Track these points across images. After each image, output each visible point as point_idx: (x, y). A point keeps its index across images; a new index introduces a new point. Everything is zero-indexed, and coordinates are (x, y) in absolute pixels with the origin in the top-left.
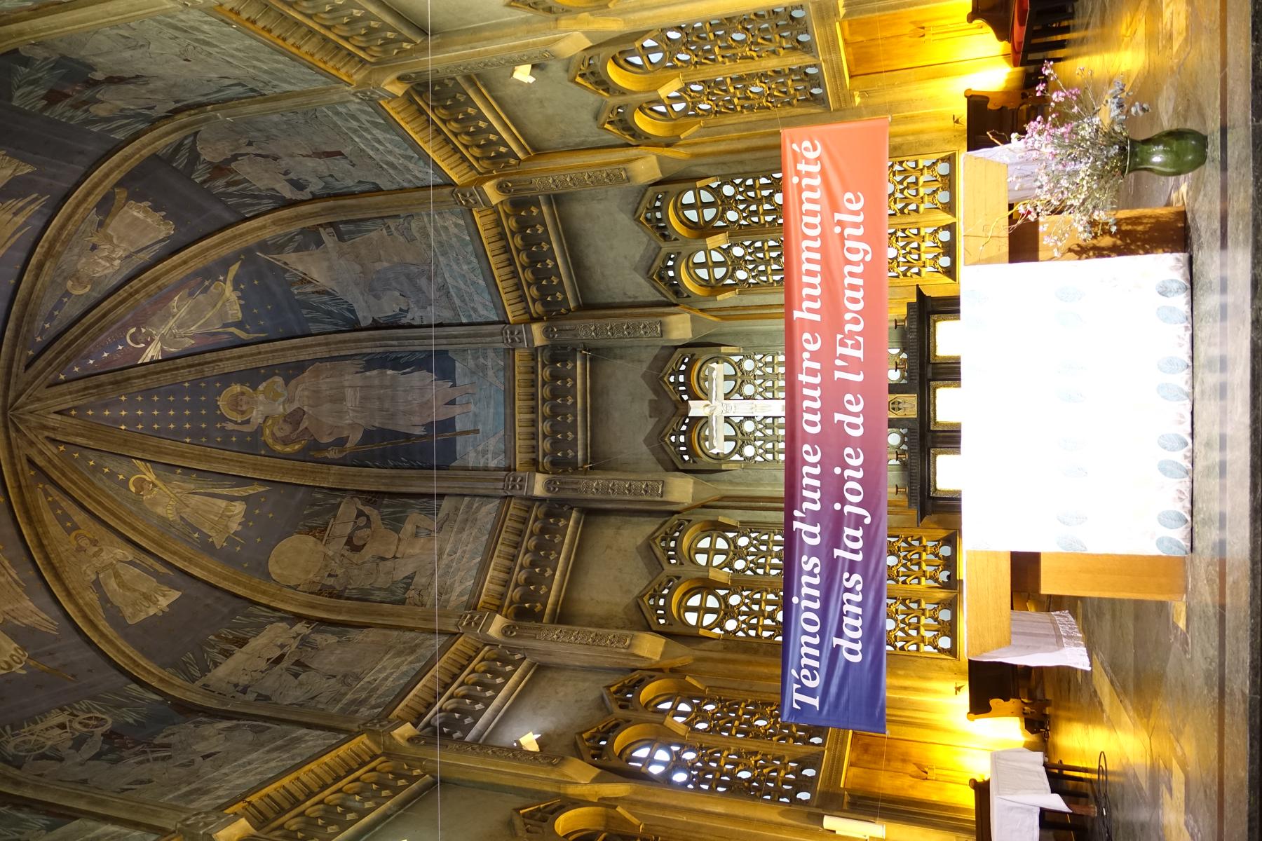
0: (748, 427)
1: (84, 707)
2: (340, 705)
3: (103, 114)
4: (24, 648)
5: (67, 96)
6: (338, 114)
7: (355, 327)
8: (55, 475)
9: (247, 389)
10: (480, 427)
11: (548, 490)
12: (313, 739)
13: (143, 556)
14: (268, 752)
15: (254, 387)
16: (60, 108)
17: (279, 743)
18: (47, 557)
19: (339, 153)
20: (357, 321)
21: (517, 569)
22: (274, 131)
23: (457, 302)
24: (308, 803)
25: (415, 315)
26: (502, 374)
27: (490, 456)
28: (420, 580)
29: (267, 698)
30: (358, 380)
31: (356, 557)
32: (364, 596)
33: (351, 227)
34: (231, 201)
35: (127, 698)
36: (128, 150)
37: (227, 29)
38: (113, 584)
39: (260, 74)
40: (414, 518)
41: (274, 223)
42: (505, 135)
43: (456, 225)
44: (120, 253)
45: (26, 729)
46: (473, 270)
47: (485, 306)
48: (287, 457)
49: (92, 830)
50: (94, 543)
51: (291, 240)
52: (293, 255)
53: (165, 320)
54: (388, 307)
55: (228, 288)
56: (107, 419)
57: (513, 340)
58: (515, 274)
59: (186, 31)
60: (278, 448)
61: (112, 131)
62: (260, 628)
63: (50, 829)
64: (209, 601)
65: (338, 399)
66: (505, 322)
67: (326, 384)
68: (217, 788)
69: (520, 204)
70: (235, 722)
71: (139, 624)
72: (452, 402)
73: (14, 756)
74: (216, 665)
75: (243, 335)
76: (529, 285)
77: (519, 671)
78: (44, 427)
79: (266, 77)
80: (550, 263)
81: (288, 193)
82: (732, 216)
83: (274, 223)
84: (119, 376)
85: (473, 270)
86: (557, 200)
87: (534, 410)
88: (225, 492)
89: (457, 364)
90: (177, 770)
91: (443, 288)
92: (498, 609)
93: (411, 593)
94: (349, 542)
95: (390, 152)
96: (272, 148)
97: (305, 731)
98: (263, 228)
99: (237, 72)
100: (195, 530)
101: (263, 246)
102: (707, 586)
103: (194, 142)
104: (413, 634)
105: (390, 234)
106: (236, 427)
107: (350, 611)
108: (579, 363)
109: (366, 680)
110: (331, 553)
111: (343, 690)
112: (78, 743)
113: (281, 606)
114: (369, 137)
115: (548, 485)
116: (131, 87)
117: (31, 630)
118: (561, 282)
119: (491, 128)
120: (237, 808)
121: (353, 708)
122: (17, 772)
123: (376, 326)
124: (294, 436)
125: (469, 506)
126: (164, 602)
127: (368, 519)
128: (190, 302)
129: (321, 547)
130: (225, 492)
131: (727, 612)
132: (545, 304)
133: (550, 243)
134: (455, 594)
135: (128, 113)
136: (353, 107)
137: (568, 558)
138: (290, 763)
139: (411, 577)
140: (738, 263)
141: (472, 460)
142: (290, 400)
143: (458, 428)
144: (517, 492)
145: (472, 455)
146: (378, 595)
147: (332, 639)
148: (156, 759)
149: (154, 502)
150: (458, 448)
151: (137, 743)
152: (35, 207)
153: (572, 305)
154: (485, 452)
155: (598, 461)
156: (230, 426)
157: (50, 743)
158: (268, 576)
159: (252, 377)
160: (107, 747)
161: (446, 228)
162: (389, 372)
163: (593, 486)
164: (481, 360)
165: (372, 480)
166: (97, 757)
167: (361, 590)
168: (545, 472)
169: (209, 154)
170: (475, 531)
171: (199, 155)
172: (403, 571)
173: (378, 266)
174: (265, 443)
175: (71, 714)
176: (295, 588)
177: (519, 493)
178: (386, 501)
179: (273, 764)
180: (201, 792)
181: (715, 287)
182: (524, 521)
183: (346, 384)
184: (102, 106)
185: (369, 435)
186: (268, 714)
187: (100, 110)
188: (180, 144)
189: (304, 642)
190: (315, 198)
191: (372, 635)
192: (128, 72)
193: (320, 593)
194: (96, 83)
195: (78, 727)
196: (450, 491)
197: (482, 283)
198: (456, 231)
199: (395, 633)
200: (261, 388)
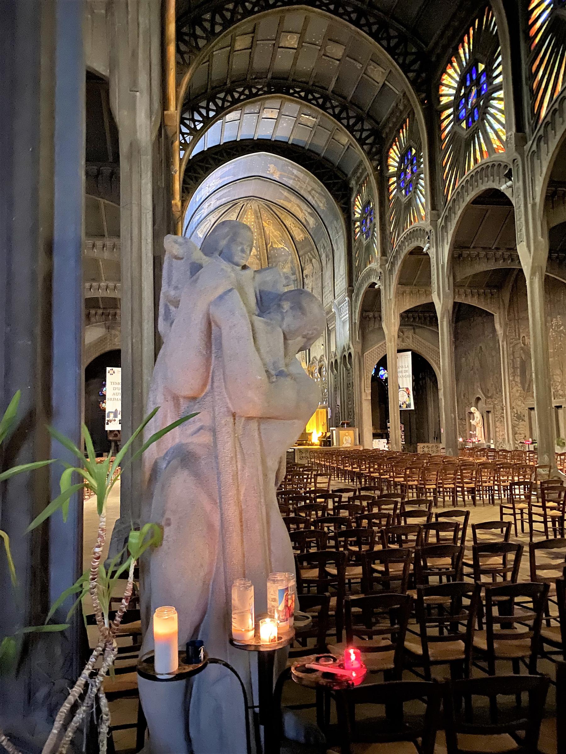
52: (289, 265)
53: (274, 229)
75: (269, 246)
84: (259, 217)
98: (297, 261)
169: (314, 260)
190: (303, 278)
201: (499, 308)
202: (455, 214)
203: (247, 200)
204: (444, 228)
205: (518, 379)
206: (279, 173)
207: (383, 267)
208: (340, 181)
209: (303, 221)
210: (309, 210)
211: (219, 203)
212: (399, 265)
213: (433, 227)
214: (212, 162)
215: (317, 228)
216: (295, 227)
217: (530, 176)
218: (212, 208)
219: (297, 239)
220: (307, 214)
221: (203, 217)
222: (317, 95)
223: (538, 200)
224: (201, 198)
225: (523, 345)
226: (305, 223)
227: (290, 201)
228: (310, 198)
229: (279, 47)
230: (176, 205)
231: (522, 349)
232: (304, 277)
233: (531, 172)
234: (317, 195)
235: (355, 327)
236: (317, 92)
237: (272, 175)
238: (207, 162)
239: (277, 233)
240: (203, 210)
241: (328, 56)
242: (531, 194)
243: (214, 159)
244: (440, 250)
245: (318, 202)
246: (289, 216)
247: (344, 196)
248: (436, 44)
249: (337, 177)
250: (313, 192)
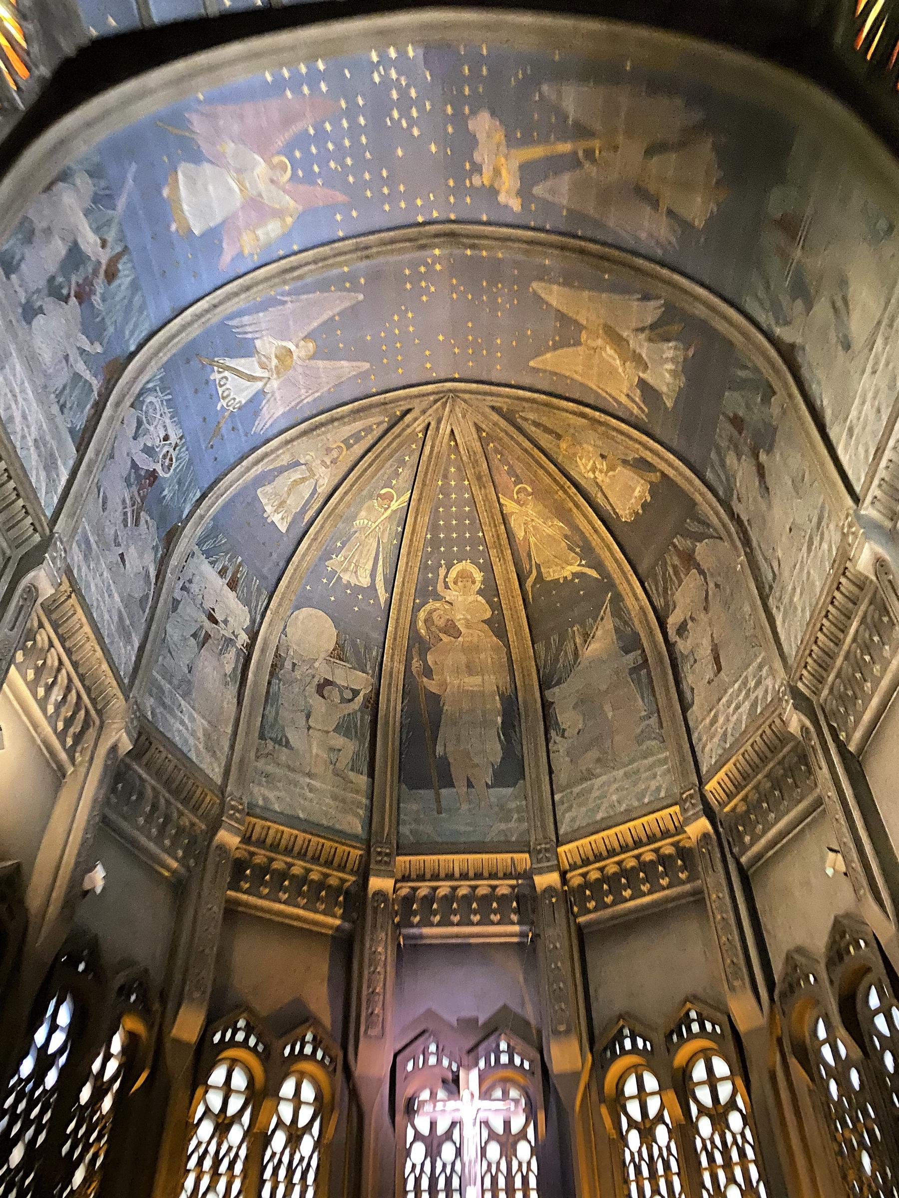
0: (448, 1151)
1: (182, 455)
2: (159, 678)
3: (728, 462)
4: (239, 408)
5: (740, 433)
6: (760, 667)
7: (544, 685)
8: (397, 430)
9: (478, 586)
11: (376, 893)
12: (126, 654)
13: (321, 500)
14: (120, 612)
15: (480, 592)
16: (728, 426)
17: (128, 622)
18: (322, 425)
19: (719, 669)
21: (289, 860)
22: (733, 607)
23: (576, 790)
24: (61, 650)
25: (560, 745)
26: (502, 838)
27: (413, 826)
28: (284, 755)
29: (175, 609)
31: (312, 689)
33: (644, 680)
34: (658, 569)
35: (187, 489)
36: (697, 482)
37: (827, 566)
38: (295, 475)
39: (787, 596)
40: (349, 747)
41: (641, 608)
42: (763, 842)
43: (658, 789)
44: (600, 477)
45: (166, 410)
46: (612, 806)
47: (573, 820)
48: (413, 623)
49: (64, 464)
50: (334, 462)
51: (626, 623)
55: (576, 569)
56: (447, 470)
57: (540, 852)
58: (612, 853)
59: (818, 528)
60: (422, 615)
61: (713, 467)
62: (246, 602)
63: (71, 431)
64: (275, 556)
65: (470, 669)
66: (559, 843)
67: (487, 657)
68: (89, 566)
70: (153, 581)
71: (256, 498)
72: (470, 785)
73: (143, 402)
74: (212, 563)
76: (601, 869)
78: (439, 421)
79: (786, 600)
80: (627, 893)
81: (673, 621)
82: (705, 1126)
83: (641, 608)
84: (486, 479)
85: (612, 806)
86: (698, 899)
88: (380, 569)
89: (511, 790)
90: (113, 532)
91: (589, 775)
92: (247, 839)
94: (328, 682)
95: (728, 720)
96: (715, 606)
97: (136, 645)
99: (786, 573)
100: (344, 544)
101: (618, 598)
103: (712, 537)
104: (226, 749)
105: (643, 719)
106: (441, 577)
107: (255, 683)
108: (516, 928)
109: (183, 702)
110: (317, 665)
111: (176, 682)
112: (149, 451)
113: (267, 619)
114: (741, 698)
115: (380, 894)
116: (757, 483)
117: (257, 413)
118: (607, 906)
120: (66, 586)
121: (155, 690)
122: (128, 404)
123: (546, 705)
124: (433, 629)
125: (359, 805)
126: (276, 518)
127: (350, 701)
128: (559, 537)
129: (323, 655)
130: (380, 569)
131: (222, 1127)
132: (582, 887)
133: (651, 892)
134: (267, 793)
135: (732, 480)
136: (769, 682)
137: (298, 918)
138: (105, 634)
139: (287, 745)
140: (647, 1136)
141: (411, 807)
143: (443, 791)
144: (374, 858)
145: (415, 807)
146: (271, 711)
147: (229, 669)
148: (125, 514)
149: (371, 509)
150: (422, 791)
151: (143, 499)
152: (636, 411)
153: (581, 920)
154: (417, 821)
156: (442, 571)
157: (152, 428)
158: (298, 607)
159: (490, 591)
160: (143, 473)
161: (655, 776)
162: (499, 719)
164: (515, 816)
166: (134, 465)
167: (277, 695)
168: (395, 891)
169: (701, 549)
170: (333, 812)
171: (701, 541)
172: (292, 736)
173: (607, 708)
175: (176, 445)
176: (284, 632)
177: (372, 861)
178: (368, 718)
179: (106, 617)
180: (87, 553)
181: (618, 1102)
182: (342, 868)
183: (486, 677)
184: (735, 461)
185: (435, 699)
186: (158, 611)
187: (731, 459)
188: (709, 526)
189: (229, 642)
191: (229, 705)
192: (770, 481)
193: (277, 655)
194: (756, 456)
195: (165, 451)
197: (599, 817)
198: (653, 788)
199: (229, 730)
200: (480, 598)
239: (554, 528)
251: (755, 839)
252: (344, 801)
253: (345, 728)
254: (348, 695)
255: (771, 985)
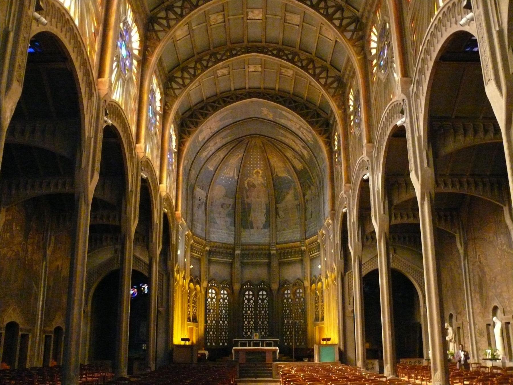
7: (277, 202)
10: (251, 236)
15: (261, 176)
20: (278, 203)
28: (216, 225)
30: (263, 202)
32: (211, 211)
40: (229, 220)
44: (292, 159)
54: (281, 213)
55: (286, 175)
60: (246, 182)
69: (302, 252)
72: (258, 229)
77: (198, 255)
81: (307, 197)
86: (302, 261)
87: (256, 250)
88: (235, 172)
91: (284, 230)
93: (212, 223)
94: (224, 204)
102: (216, 294)
115: (238, 254)
118: (285, 259)
119: (315, 253)
123: (277, 208)
125: (232, 234)
142: (258, 184)
143: (252, 230)
147: (203, 210)
155: (243, 265)
162: (265, 211)
163: (237, 265)
165: (239, 207)
169: (312, 187)
174: (246, 179)
178: (233, 211)
182: (230, 249)
185: (249, 205)
196: (236, 229)
197: (285, 240)
201: (459, 229)
202: (382, 145)
203: (251, 137)
204: (378, 158)
205: (478, 296)
206: (271, 115)
207: (347, 193)
208: (322, 119)
209: (300, 153)
210: (302, 144)
211: (224, 141)
212: (357, 191)
213: (369, 157)
214: (210, 109)
215: (311, 159)
216: (294, 158)
217: (415, 113)
218: (219, 145)
219: (298, 168)
220: (301, 147)
221: (211, 153)
222: (287, 52)
223: (422, 133)
224: (204, 138)
225: (479, 263)
226: (302, 155)
227: (286, 137)
228: (300, 134)
229: (248, 19)
230: (141, 148)
231: (479, 266)
232: (306, 202)
233: (416, 109)
234: (305, 131)
235: (337, 248)
236: (287, 50)
237: (266, 115)
238: (207, 110)
239: (281, 164)
240: (210, 148)
241: (289, 23)
242: (417, 129)
243: (213, 107)
244: (376, 177)
245: (307, 137)
246: (288, 150)
247: (326, 132)
248: (364, 9)
249: (318, 115)
250: (302, 129)
251: (313, 254)
252: (229, 234)
253: (228, 215)
254: (228, 206)
255: (311, 280)
